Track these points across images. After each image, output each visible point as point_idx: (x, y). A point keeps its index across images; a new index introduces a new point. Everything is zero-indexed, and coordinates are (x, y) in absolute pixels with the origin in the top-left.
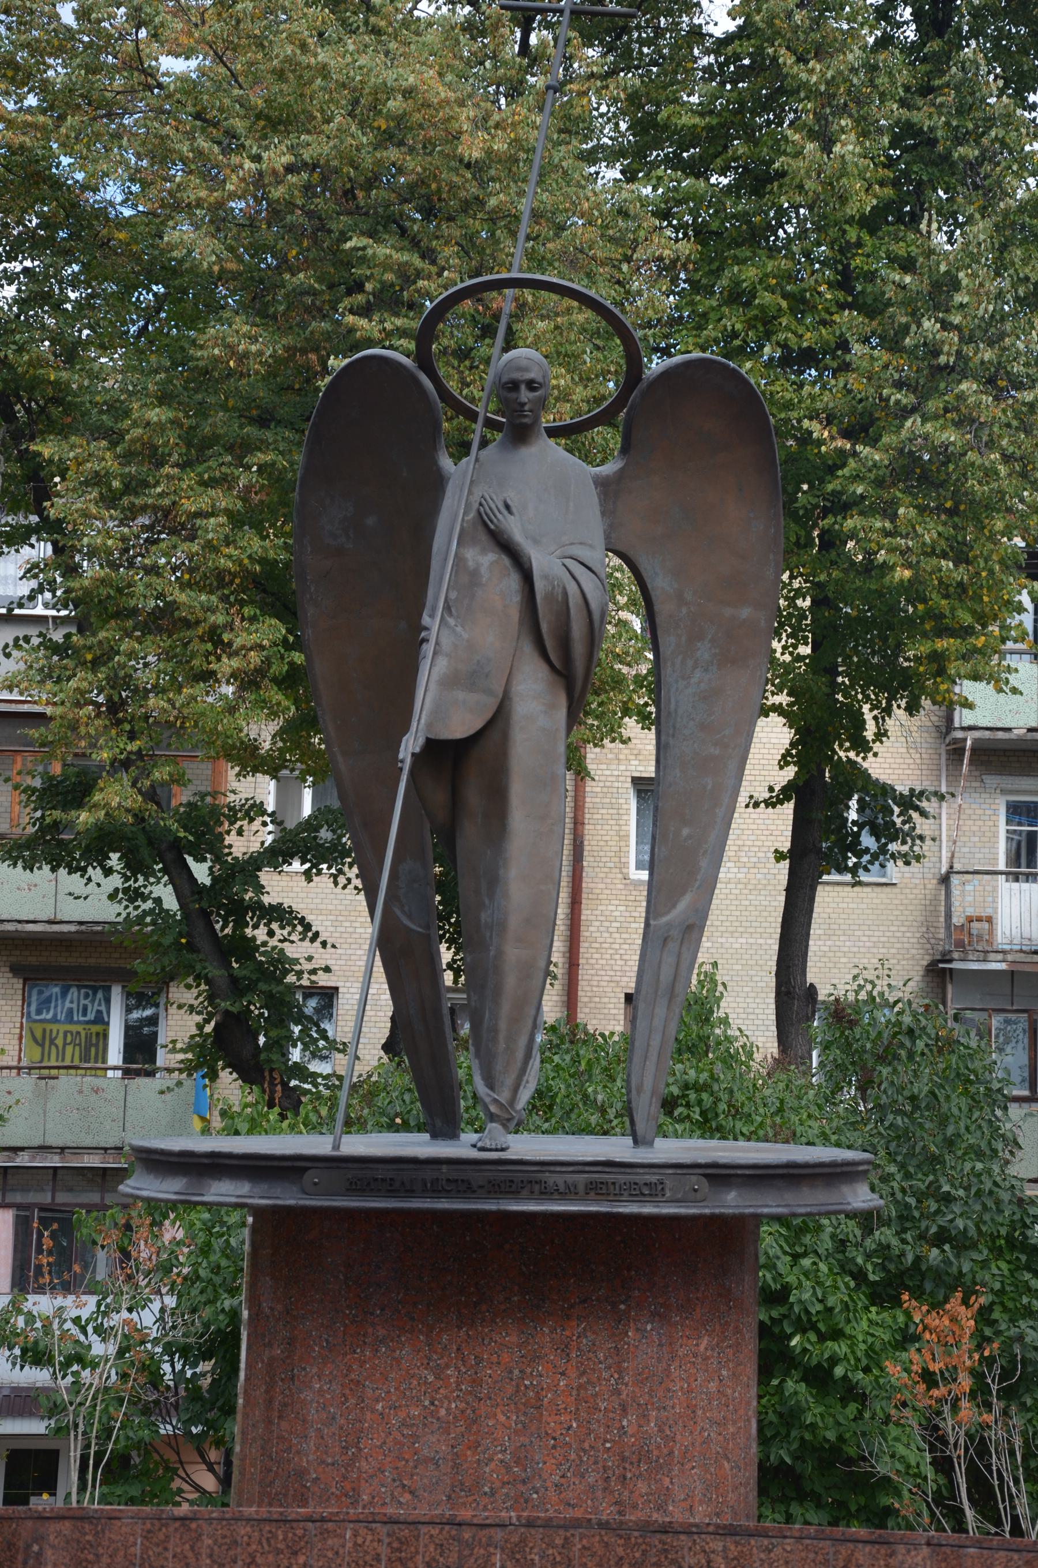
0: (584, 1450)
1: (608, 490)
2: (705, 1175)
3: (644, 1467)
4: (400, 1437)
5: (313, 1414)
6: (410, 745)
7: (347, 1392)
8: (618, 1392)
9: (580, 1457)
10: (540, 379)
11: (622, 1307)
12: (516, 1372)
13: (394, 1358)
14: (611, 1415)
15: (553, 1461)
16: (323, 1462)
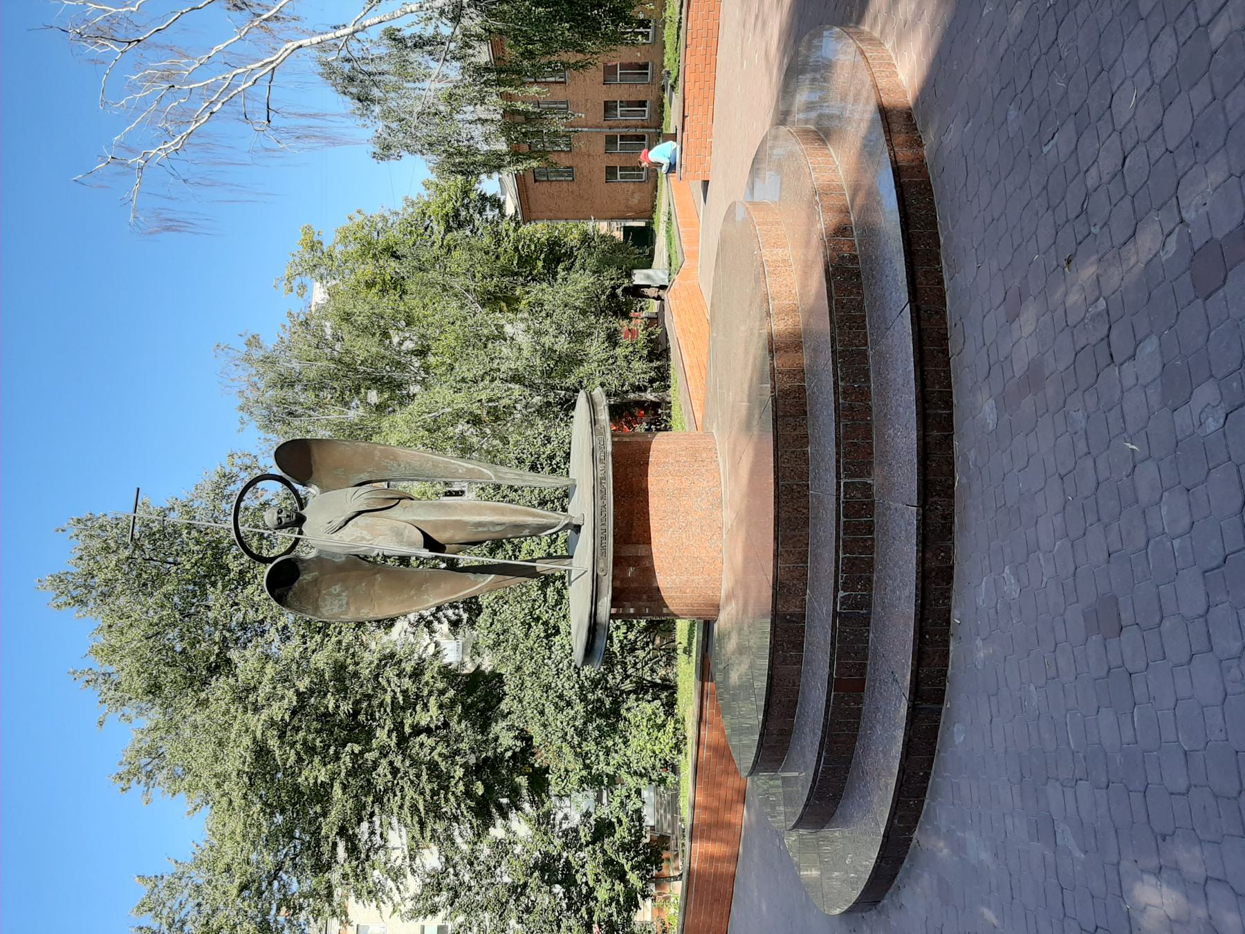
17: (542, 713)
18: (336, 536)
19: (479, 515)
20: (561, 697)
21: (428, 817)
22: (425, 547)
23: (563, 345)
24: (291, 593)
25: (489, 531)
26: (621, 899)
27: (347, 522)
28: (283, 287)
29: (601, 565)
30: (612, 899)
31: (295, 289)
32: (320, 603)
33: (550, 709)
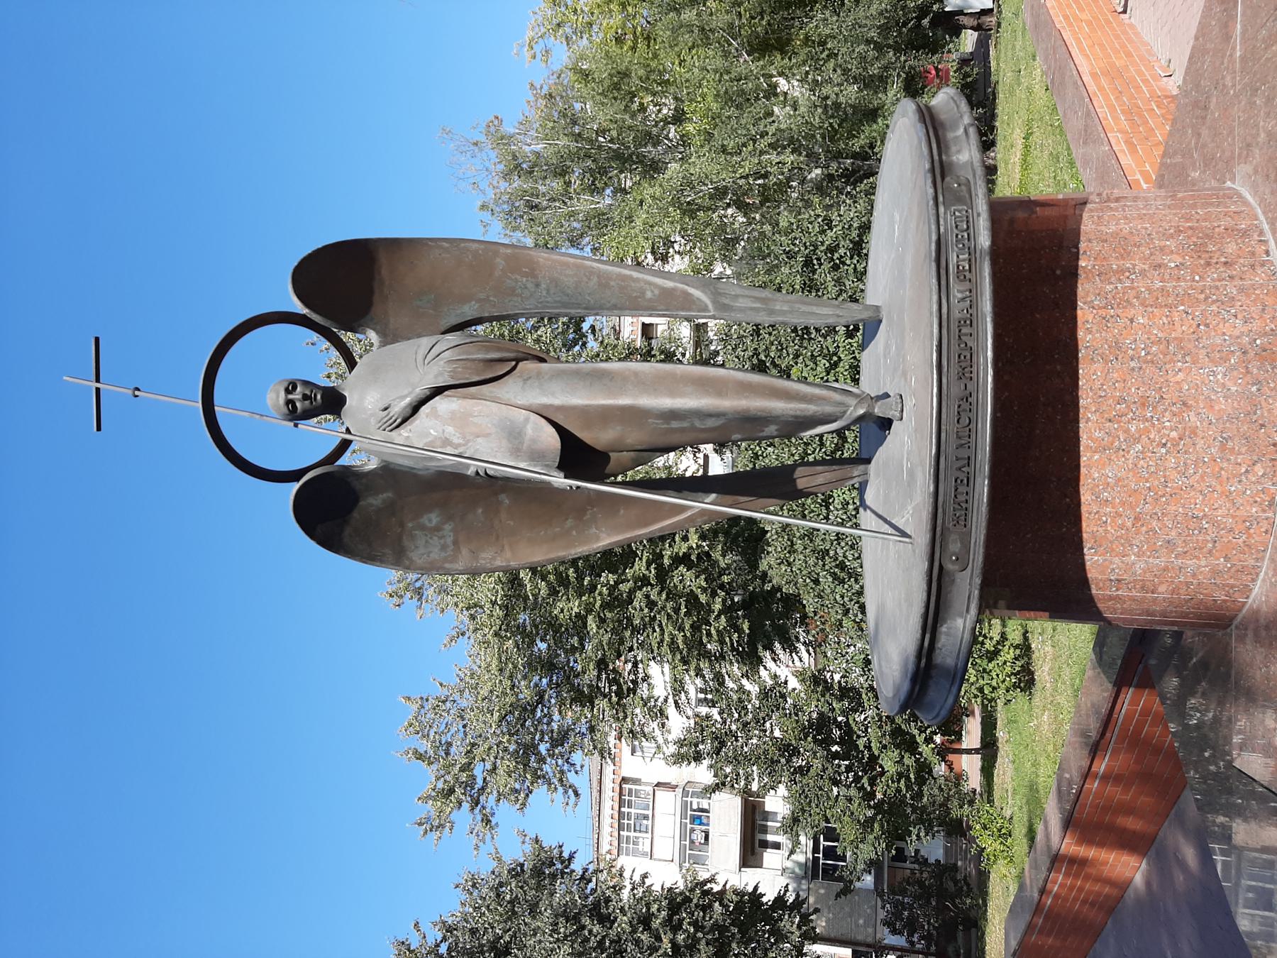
0: (1206, 298)
1: (389, 338)
3: (1211, 248)
4: (1197, 477)
5: (1161, 562)
6: (559, 480)
8: (1143, 272)
9: (1214, 302)
10: (286, 384)
11: (1058, 272)
12: (1133, 364)
14: (1167, 277)
15: (1221, 325)
16: (1210, 552)
17: (817, 582)
19: (672, 394)
20: (842, 566)
21: (691, 653)
22: (561, 467)
24: (348, 531)
25: (693, 429)
26: (912, 776)
27: (415, 408)
28: (527, 54)
29: (954, 546)
30: (900, 775)
31: (539, 56)
32: (406, 542)
33: (826, 581)
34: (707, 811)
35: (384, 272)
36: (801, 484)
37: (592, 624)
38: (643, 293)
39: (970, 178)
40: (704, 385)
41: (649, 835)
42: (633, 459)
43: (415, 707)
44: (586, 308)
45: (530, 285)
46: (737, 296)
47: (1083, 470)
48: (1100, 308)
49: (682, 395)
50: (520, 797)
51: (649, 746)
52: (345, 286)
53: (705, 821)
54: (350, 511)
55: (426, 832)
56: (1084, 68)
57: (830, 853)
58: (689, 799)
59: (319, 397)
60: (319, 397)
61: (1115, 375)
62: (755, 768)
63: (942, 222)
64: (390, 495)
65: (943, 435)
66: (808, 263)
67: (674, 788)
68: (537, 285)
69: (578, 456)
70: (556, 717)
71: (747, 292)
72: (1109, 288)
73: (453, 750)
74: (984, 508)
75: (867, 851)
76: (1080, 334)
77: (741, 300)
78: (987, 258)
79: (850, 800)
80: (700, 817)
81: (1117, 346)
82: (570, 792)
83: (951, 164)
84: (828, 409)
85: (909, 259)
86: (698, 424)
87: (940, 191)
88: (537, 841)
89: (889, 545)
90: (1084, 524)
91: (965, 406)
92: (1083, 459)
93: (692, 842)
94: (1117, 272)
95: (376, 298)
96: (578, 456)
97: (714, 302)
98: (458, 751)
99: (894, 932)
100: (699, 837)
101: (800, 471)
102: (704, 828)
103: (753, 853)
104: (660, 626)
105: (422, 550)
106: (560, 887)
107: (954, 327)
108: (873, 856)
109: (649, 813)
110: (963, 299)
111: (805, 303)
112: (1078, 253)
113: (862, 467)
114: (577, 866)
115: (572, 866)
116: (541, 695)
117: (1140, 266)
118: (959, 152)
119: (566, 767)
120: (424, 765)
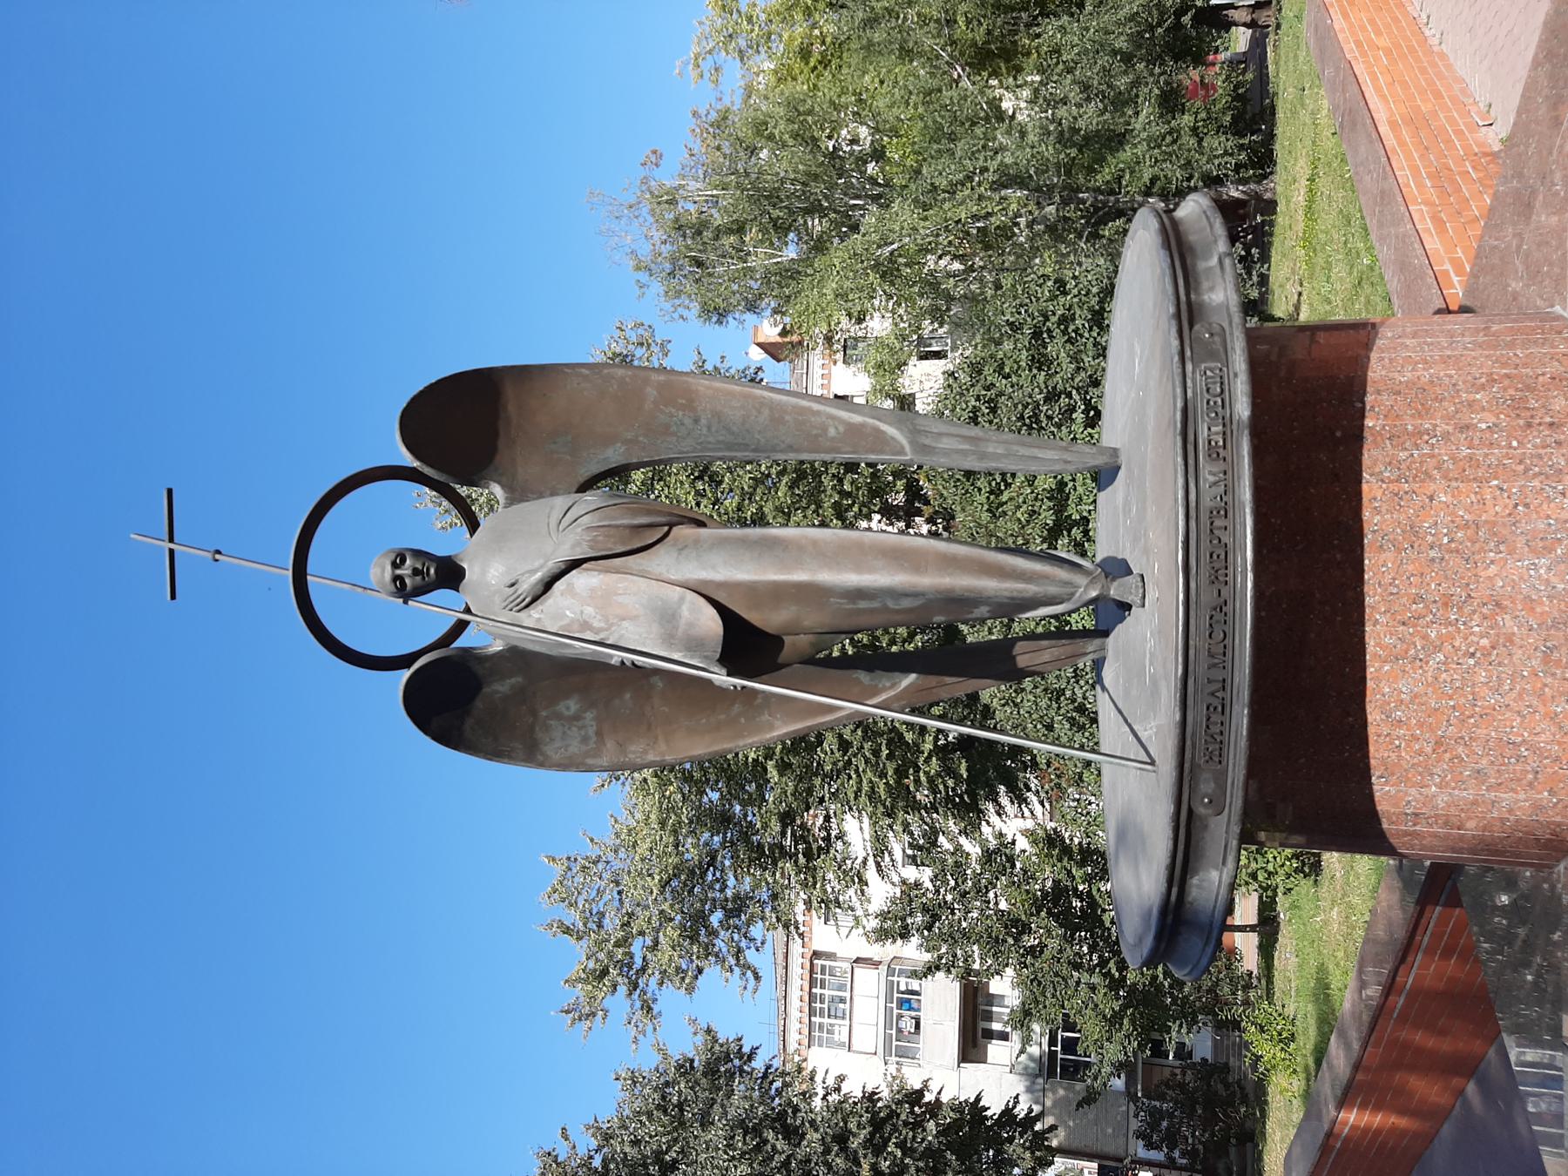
0: (1526, 470)
1: (517, 494)
2: (1191, 326)
3: (1533, 403)
4: (1514, 694)
5: (1469, 795)
6: (721, 678)
7: (1447, 756)
8: (1446, 436)
9: (1536, 476)
10: (393, 556)
11: (1338, 434)
12: (1432, 554)
13: (1412, 702)
14: (1476, 442)
15: (1545, 506)
16: (1530, 784)
18: (533, 616)
19: (858, 569)
20: (1081, 709)
21: (895, 803)
23: (1090, 117)
24: (469, 722)
25: (886, 609)
27: (548, 585)
29: (1207, 786)
32: (539, 735)
34: (917, 993)
35: (511, 408)
36: (1022, 661)
37: (773, 774)
38: (825, 430)
39: (1226, 325)
40: (897, 557)
41: (847, 1022)
42: (812, 644)
43: (559, 869)
44: (755, 450)
45: (687, 421)
46: (940, 434)
47: (1370, 684)
48: (1391, 482)
49: (871, 570)
50: (688, 979)
51: (846, 920)
52: (464, 429)
53: (915, 1005)
54: (472, 699)
55: (573, 1023)
56: (1381, 116)
57: (1070, 1046)
58: (895, 979)
59: (432, 571)
60: (432, 571)
61: (1411, 568)
62: (975, 948)
63: (1189, 383)
64: (520, 679)
65: (1192, 652)
66: (1037, 335)
67: (876, 964)
68: (696, 421)
69: (747, 646)
70: (731, 882)
71: (953, 430)
72: (1403, 455)
73: (606, 921)
74: (1243, 743)
75: (1113, 1052)
76: (1366, 514)
77: (945, 440)
78: (1246, 432)
79: (1093, 988)
80: (909, 1001)
81: (1413, 531)
82: (749, 973)
83: (1201, 305)
84: (1053, 590)
85: (1151, 411)
86: (891, 604)
87: (1187, 342)
88: (709, 1031)
89: (1130, 754)
90: (1372, 749)
91: (1218, 616)
92: (1370, 670)
93: (899, 1031)
94: (1412, 434)
95: (501, 443)
96: (747, 646)
97: (911, 443)
98: (612, 923)
99: (1150, 1145)
100: (907, 1025)
101: (1020, 647)
102: (913, 1014)
103: (975, 1045)
104: (857, 771)
105: (557, 744)
106: (739, 1087)
107: (1204, 517)
108: (1122, 1057)
109: (847, 995)
110: (1215, 483)
111: (1024, 445)
112: (1363, 408)
113: (1097, 642)
114: (758, 1064)
115: (753, 1064)
116: (713, 856)
117: (1443, 427)
118: (1212, 289)
119: (743, 944)
120: (571, 940)
